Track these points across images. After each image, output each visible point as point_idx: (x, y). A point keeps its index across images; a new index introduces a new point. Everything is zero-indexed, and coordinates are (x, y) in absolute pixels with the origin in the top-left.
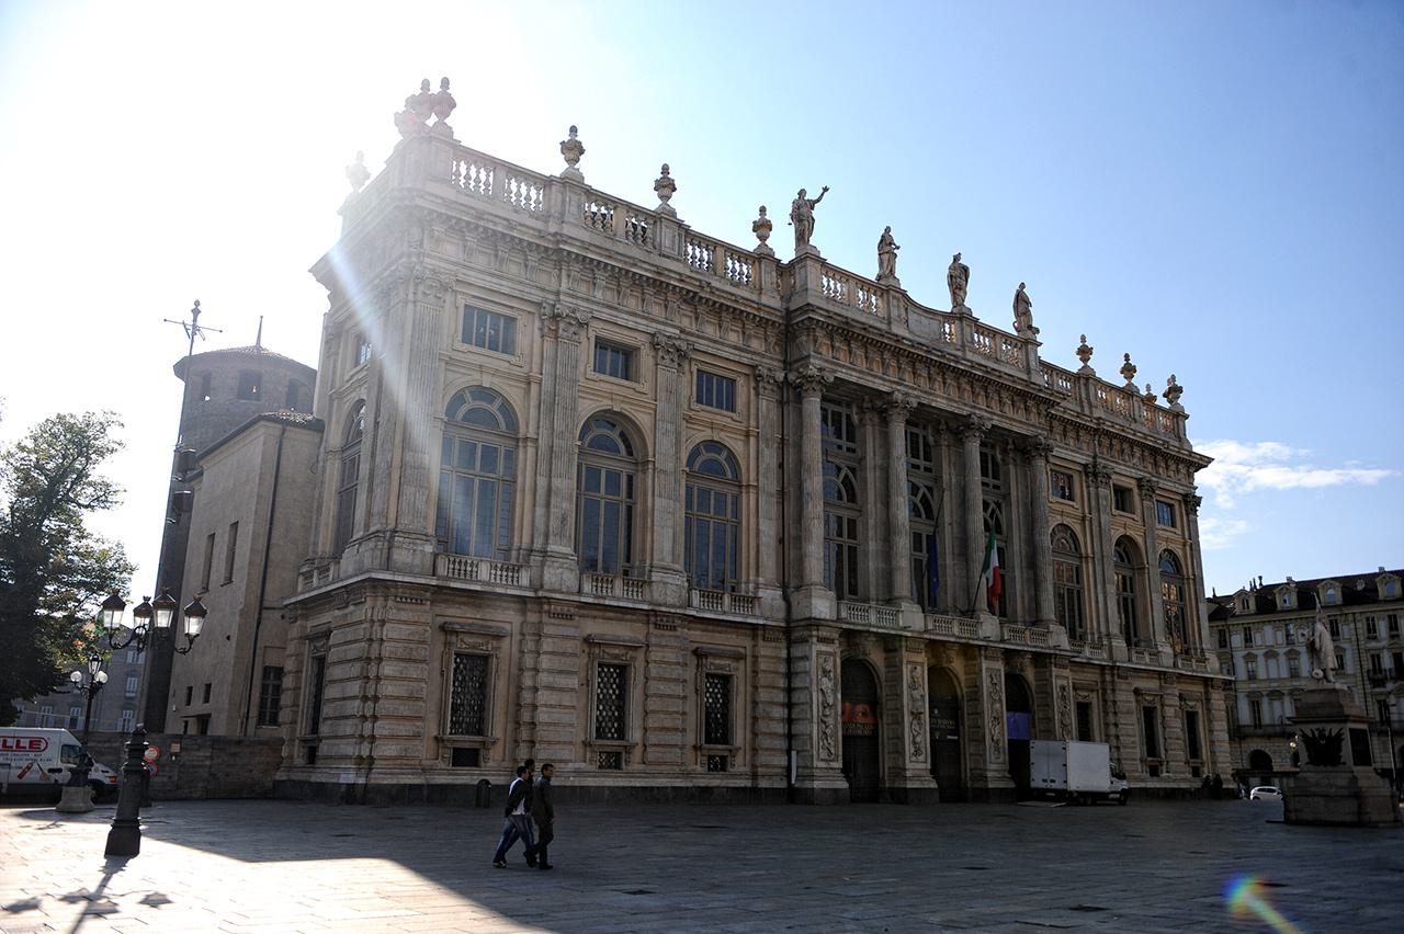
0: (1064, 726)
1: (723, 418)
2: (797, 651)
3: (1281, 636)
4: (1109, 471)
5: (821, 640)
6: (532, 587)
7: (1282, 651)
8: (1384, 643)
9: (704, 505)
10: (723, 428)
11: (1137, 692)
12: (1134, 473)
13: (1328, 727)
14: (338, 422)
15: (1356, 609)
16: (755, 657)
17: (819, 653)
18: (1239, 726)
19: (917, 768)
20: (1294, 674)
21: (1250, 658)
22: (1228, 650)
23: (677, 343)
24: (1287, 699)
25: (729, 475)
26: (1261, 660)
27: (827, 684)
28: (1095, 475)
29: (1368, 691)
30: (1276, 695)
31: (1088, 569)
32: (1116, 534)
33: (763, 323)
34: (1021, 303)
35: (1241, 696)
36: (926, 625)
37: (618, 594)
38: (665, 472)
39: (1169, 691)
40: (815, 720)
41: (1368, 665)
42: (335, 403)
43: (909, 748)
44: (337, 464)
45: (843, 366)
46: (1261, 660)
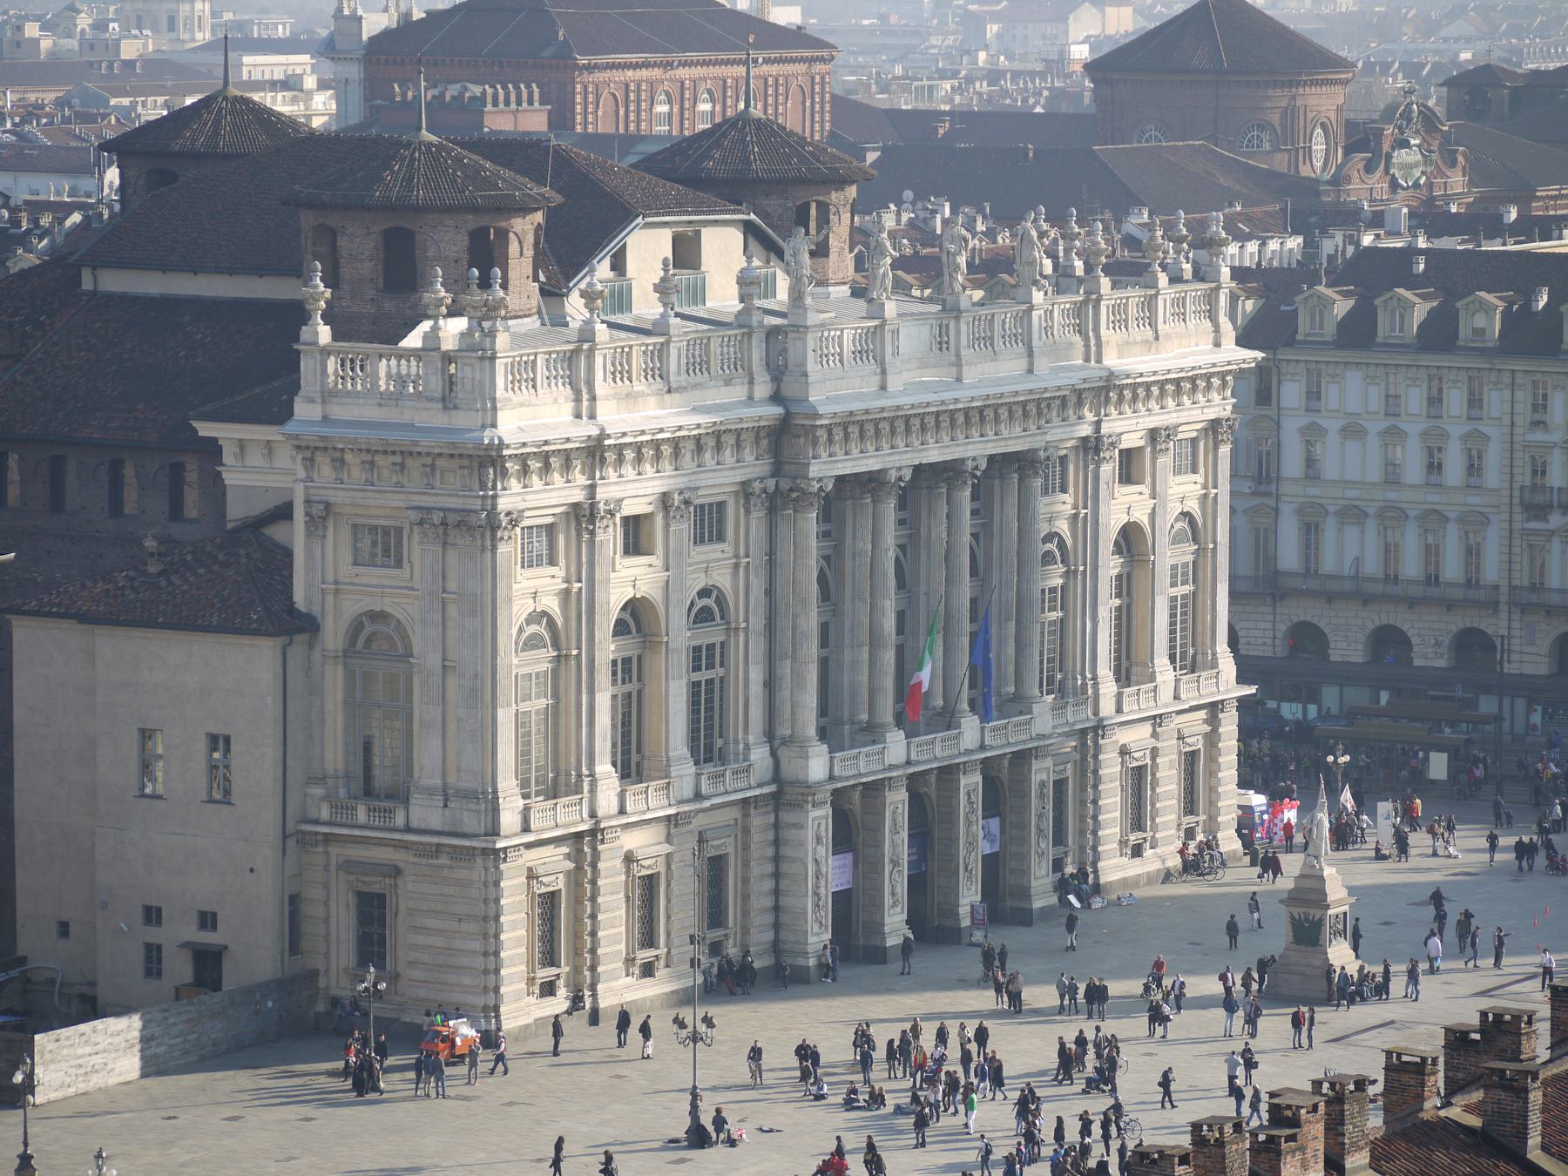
0: (1039, 830)
2: (788, 817)
3: (1376, 400)
7: (1375, 426)
8: (1556, 436)
13: (1312, 912)
14: (335, 621)
15: (1519, 366)
16: (746, 831)
18: (1277, 572)
19: (895, 924)
20: (1392, 476)
21: (1312, 434)
22: (1272, 412)
24: (1371, 526)
26: (1333, 439)
28: (1097, 450)
29: (1517, 526)
30: (1352, 514)
35: (1287, 510)
36: (908, 754)
41: (1524, 478)
42: (330, 599)
43: (888, 900)
44: (340, 670)
46: (1333, 439)
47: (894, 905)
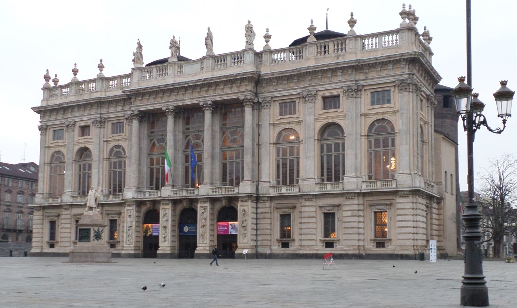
1: (120, 136)
4: (313, 93)
5: (129, 206)
6: (62, 202)
9: (115, 167)
10: (119, 140)
11: (321, 207)
12: (339, 85)
17: (128, 210)
23: (97, 119)
25: (123, 154)
27: (128, 219)
31: (301, 147)
32: (319, 125)
33: (124, 100)
34: (250, 31)
37: (79, 201)
38: (96, 161)
39: (348, 203)
40: (125, 232)
45: (143, 105)
47: (165, 241)
